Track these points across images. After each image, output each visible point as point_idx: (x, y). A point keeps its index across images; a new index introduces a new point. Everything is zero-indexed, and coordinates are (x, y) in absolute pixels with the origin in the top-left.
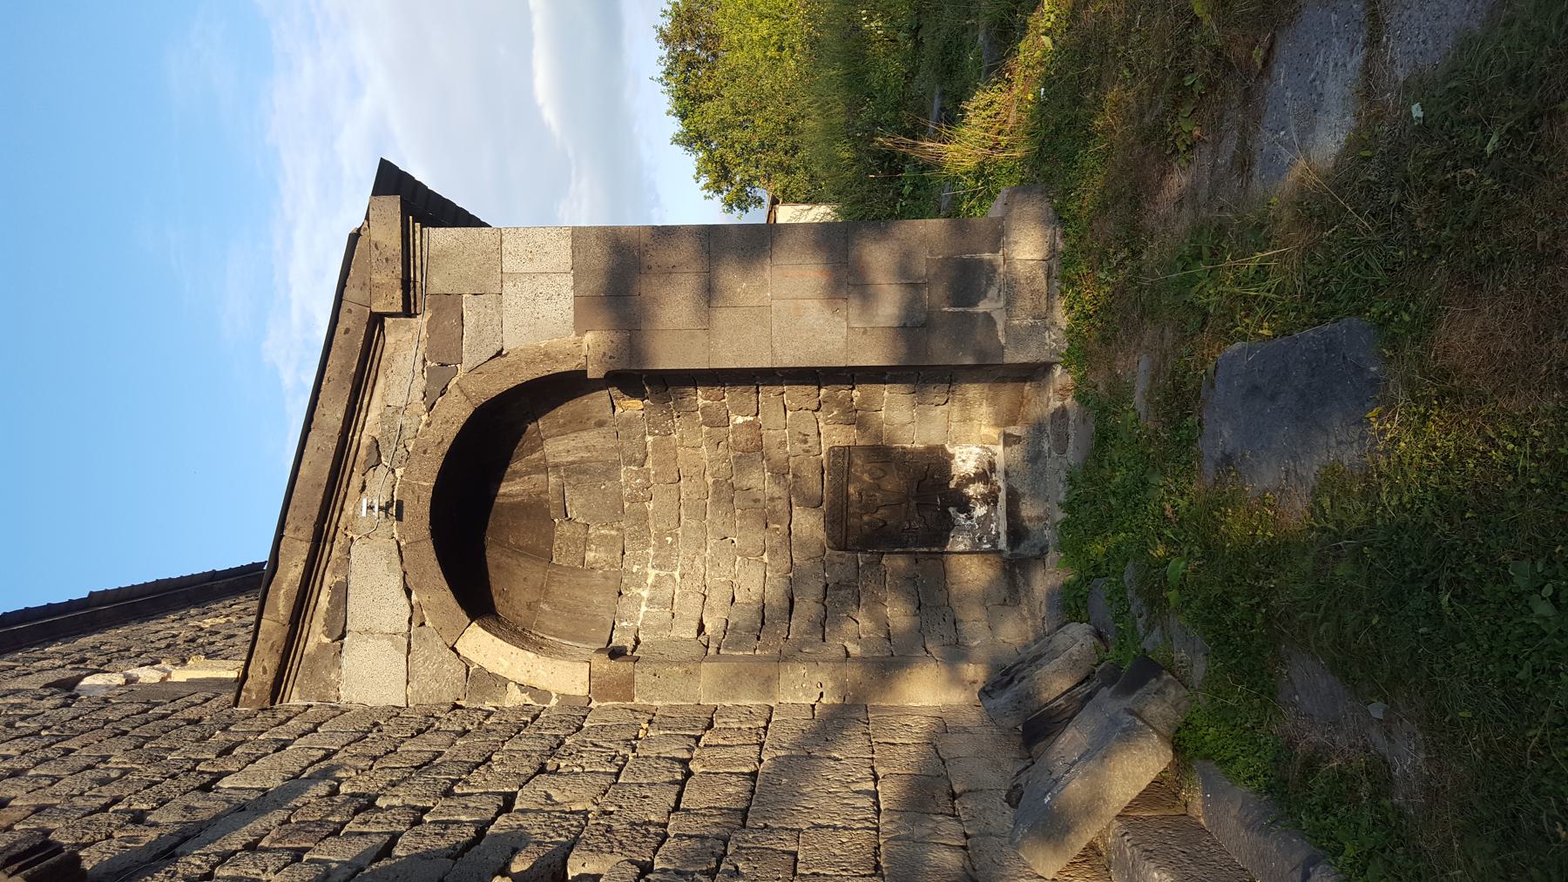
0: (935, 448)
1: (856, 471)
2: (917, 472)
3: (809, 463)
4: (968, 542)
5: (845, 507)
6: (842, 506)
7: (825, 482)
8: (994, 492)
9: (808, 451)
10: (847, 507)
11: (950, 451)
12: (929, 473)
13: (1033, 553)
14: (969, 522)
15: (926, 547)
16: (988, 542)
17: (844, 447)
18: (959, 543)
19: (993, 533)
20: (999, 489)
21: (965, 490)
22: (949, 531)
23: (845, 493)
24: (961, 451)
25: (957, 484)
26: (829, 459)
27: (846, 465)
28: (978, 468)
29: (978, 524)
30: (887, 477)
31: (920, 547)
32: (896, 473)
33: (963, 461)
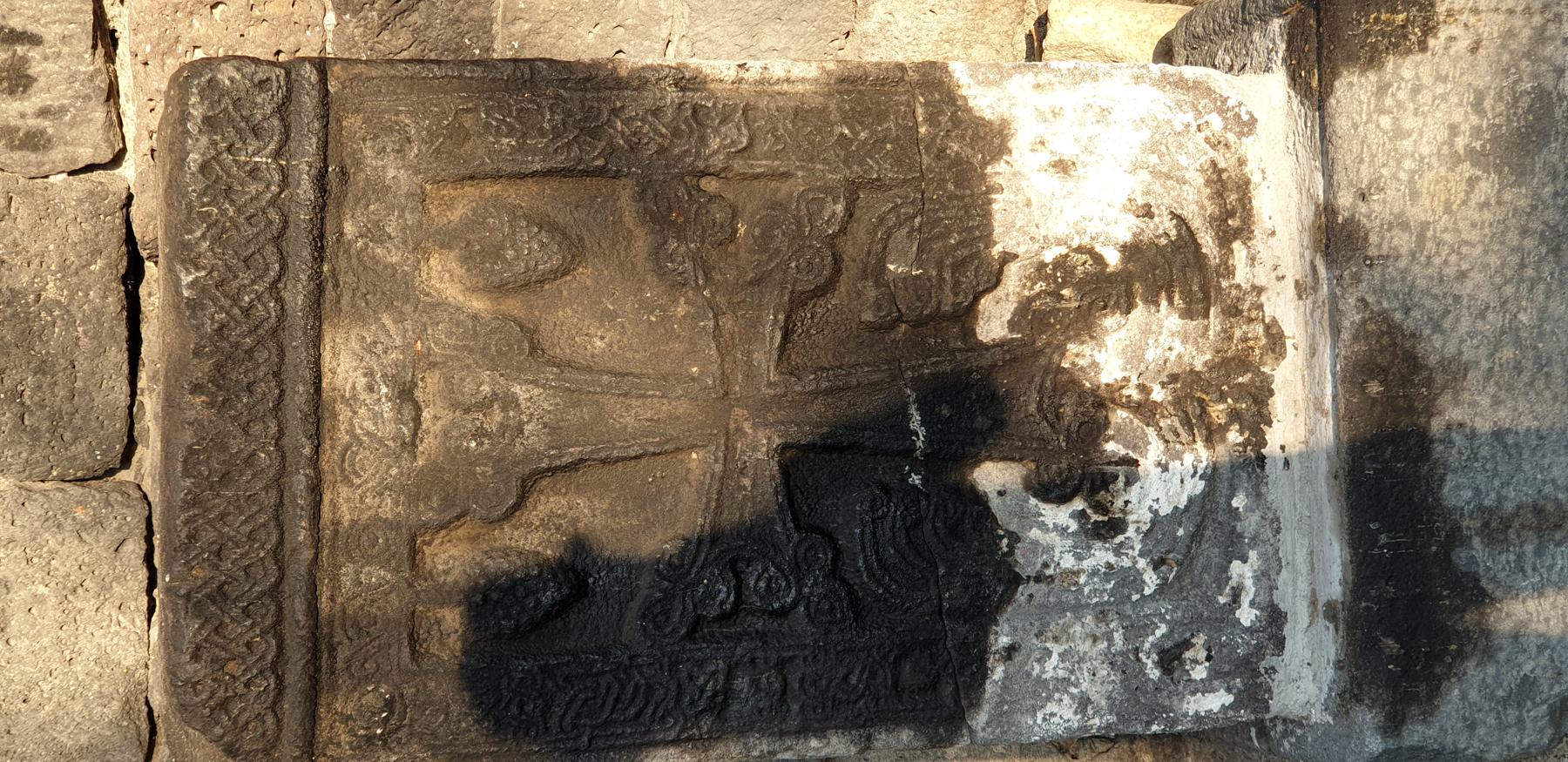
0: (880, 82)
1: (375, 233)
2: (780, 241)
3: (48, 212)
4: (1098, 683)
5: (299, 482)
6: (279, 483)
7: (149, 331)
8: (1243, 362)
9: (34, 141)
10: (316, 489)
11: (983, 100)
12: (851, 249)
13: (1512, 737)
14: (1101, 555)
15: (845, 726)
16: (1218, 675)
17: (288, 68)
18: (1044, 690)
19: (1247, 615)
20: (1276, 341)
21: (1078, 354)
22: (982, 614)
23: (299, 394)
24: (1046, 100)
25: (1026, 315)
26: (173, 189)
27: (305, 189)
28: (1148, 212)
29: (1157, 565)
30: (584, 274)
31: (803, 731)
32: (642, 244)
33: (1062, 166)
